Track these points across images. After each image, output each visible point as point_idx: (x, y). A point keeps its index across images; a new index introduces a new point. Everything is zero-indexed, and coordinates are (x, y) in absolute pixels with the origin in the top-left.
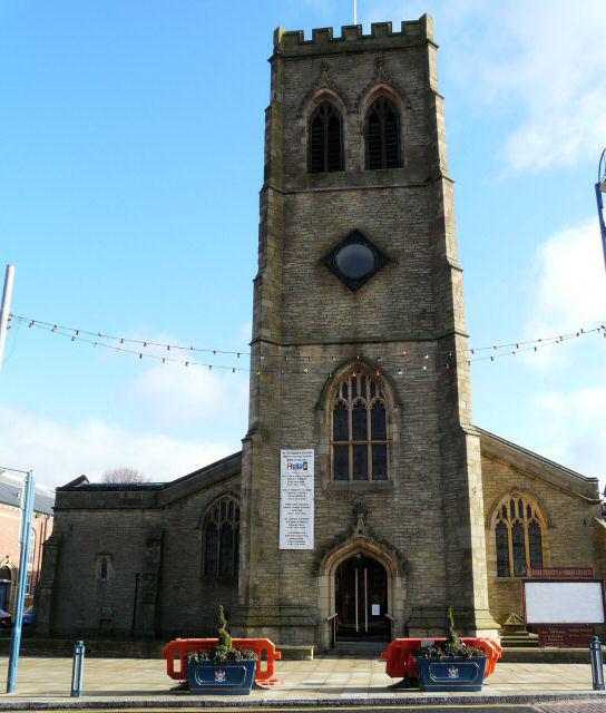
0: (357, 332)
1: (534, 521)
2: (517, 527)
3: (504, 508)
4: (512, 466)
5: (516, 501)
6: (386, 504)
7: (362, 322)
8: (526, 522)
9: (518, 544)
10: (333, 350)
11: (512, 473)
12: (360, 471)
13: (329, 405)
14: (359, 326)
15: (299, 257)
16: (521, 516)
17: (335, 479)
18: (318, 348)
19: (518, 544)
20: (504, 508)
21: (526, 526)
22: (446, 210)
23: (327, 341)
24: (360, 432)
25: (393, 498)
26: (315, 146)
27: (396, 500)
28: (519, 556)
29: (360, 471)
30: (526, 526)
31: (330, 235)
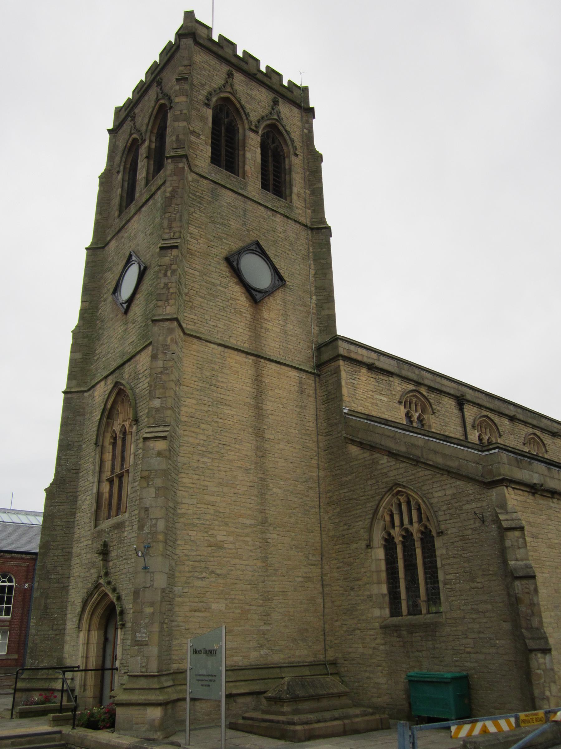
1: (426, 527)
2: (408, 536)
3: (392, 516)
4: (392, 454)
5: (402, 499)
8: (415, 529)
9: (411, 567)
11: (392, 462)
13: (108, 440)
14: (125, 348)
16: (411, 522)
18: (102, 383)
19: (411, 567)
20: (392, 516)
21: (417, 536)
25: (125, 531)
27: (126, 534)
28: (412, 580)
30: (417, 536)
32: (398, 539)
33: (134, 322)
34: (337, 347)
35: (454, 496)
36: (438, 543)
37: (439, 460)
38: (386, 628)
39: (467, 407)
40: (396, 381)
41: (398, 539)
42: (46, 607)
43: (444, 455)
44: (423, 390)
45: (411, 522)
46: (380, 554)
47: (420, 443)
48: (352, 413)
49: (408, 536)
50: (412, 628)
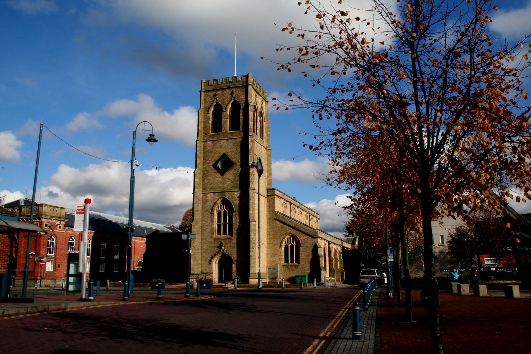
0: (223, 189)
2: (292, 246)
6: (230, 243)
7: (225, 185)
10: (216, 194)
12: (225, 233)
13: (215, 212)
15: (208, 164)
16: (293, 242)
17: (218, 234)
22: (250, 147)
23: (215, 191)
24: (225, 220)
26: (214, 123)
29: (225, 233)
31: (217, 156)
32: (289, 246)
33: (228, 179)
34: (274, 192)
35: (306, 238)
36: (301, 248)
37: (303, 230)
38: (284, 266)
39: (292, 205)
40: (282, 199)
41: (289, 246)
42: (195, 257)
43: (305, 229)
44: (285, 201)
45: (293, 242)
46: (283, 249)
47: (299, 225)
48: (278, 212)
49: (292, 246)
50: (291, 266)
